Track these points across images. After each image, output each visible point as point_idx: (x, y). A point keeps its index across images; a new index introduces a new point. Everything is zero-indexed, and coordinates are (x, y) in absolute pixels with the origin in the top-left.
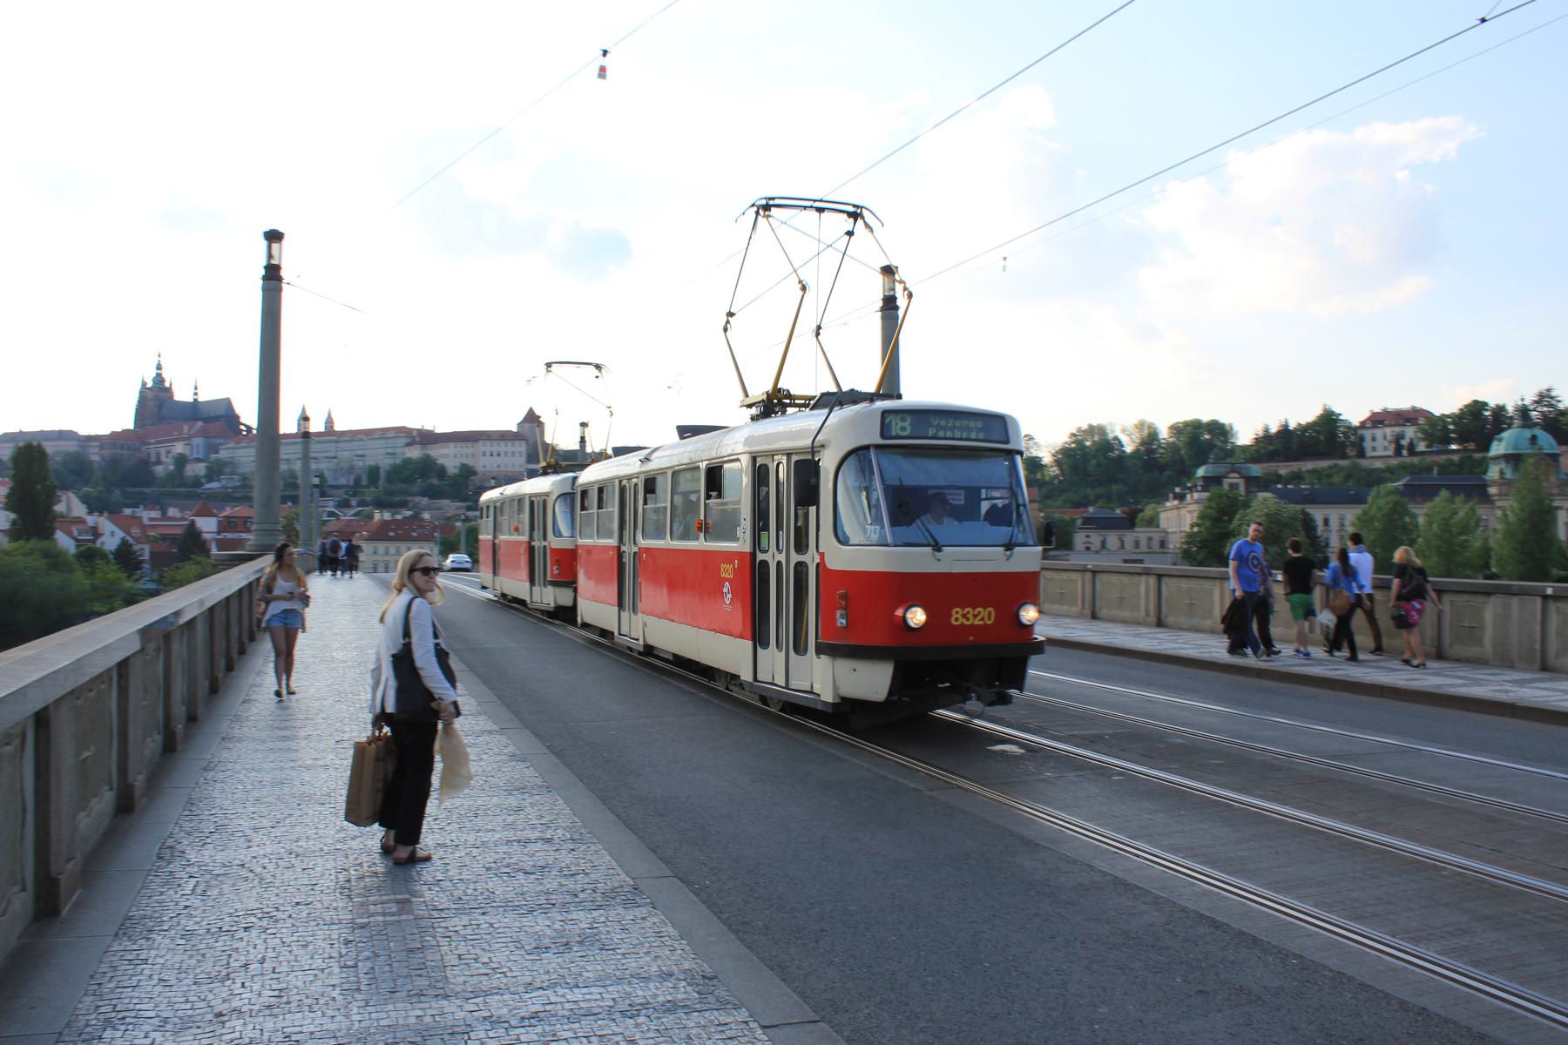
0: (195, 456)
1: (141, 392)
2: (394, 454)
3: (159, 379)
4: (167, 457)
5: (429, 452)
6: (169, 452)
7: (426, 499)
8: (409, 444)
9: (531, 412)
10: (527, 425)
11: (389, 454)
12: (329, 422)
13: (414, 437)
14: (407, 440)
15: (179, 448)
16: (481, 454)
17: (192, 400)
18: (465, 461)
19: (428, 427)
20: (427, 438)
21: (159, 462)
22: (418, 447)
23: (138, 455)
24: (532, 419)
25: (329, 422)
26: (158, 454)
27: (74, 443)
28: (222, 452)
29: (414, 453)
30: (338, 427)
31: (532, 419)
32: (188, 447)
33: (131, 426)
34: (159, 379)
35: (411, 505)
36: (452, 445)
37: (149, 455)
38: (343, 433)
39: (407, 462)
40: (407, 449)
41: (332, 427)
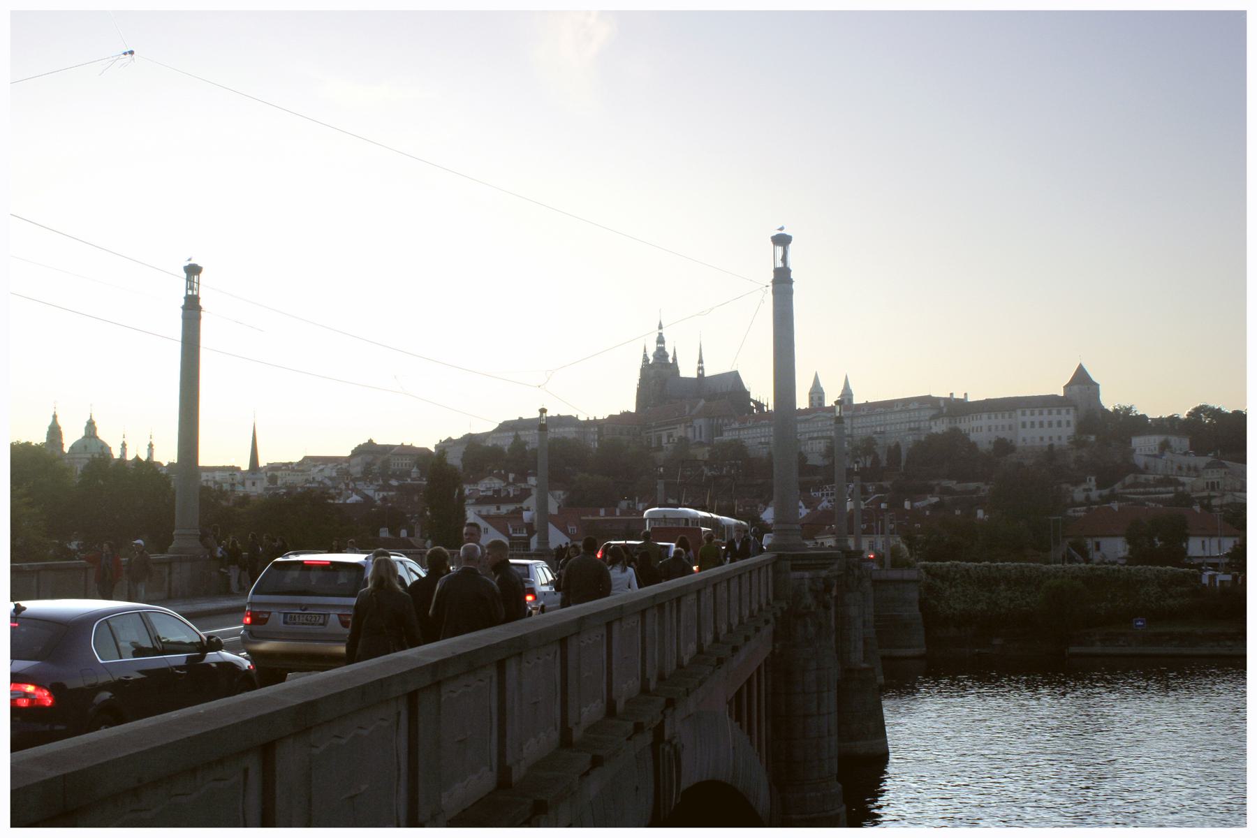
0: (698, 439)
1: (642, 370)
2: (918, 429)
3: (661, 353)
4: (669, 441)
5: (958, 425)
6: (670, 436)
7: (955, 482)
8: (934, 417)
9: (1080, 364)
10: (1075, 388)
11: (910, 429)
12: (847, 394)
13: (940, 409)
14: (933, 412)
15: (679, 432)
16: (1020, 424)
17: (695, 376)
18: (1002, 435)
19: (959, 395)
20: (956, 408)
21: (660, 448)
22: (946, 420)
24: (1082, 379)
25: (847, 394)
27: (573, 429)
28: (726, 434)
29: (940, 427)
30: (858, 400)
31: (1082, 379)
32: (689, 429)
33: (633, 409)
34: (661, 353)
35: (937, 489)
36: (985, 416)
38: (859, 406)
39: (933, 438)
40: (933, 423)
41: (850, 400)
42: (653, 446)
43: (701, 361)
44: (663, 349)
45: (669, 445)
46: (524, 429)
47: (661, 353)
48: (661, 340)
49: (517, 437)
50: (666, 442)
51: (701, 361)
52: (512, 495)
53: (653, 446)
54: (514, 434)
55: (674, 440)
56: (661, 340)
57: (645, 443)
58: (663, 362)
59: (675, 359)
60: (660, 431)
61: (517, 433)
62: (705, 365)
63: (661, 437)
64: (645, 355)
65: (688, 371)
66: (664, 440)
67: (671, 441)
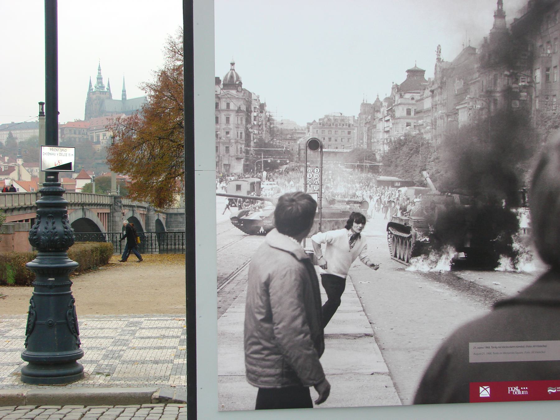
4: (104, 138)
21: (98, 142)
23: (85, 137)
26: (98, 137)
33: (83, 119)
37: (92, 138)
42: (95, 141)
43: (124, 91)
44: (101, 83)
45: (103, 141)
46: (15, 129)
47: (100, 85)
48: (100, 79)
49: (10, 135)
50: (102, 139)
51: (124, 91)
52: (3, 170)
53: (95, 141)
54: (8, 132)
55: (106, 138)
56: (100, 79)
57: (90, 139)
58: (101, 90)
59: (109, 89)
60: (99, 132)
61: (10, 132)
62: (127, 93)
63: (99, 136)
64: (90, 86)
65: (117, 96)
66: (101, 138)
67: (105, 138)
